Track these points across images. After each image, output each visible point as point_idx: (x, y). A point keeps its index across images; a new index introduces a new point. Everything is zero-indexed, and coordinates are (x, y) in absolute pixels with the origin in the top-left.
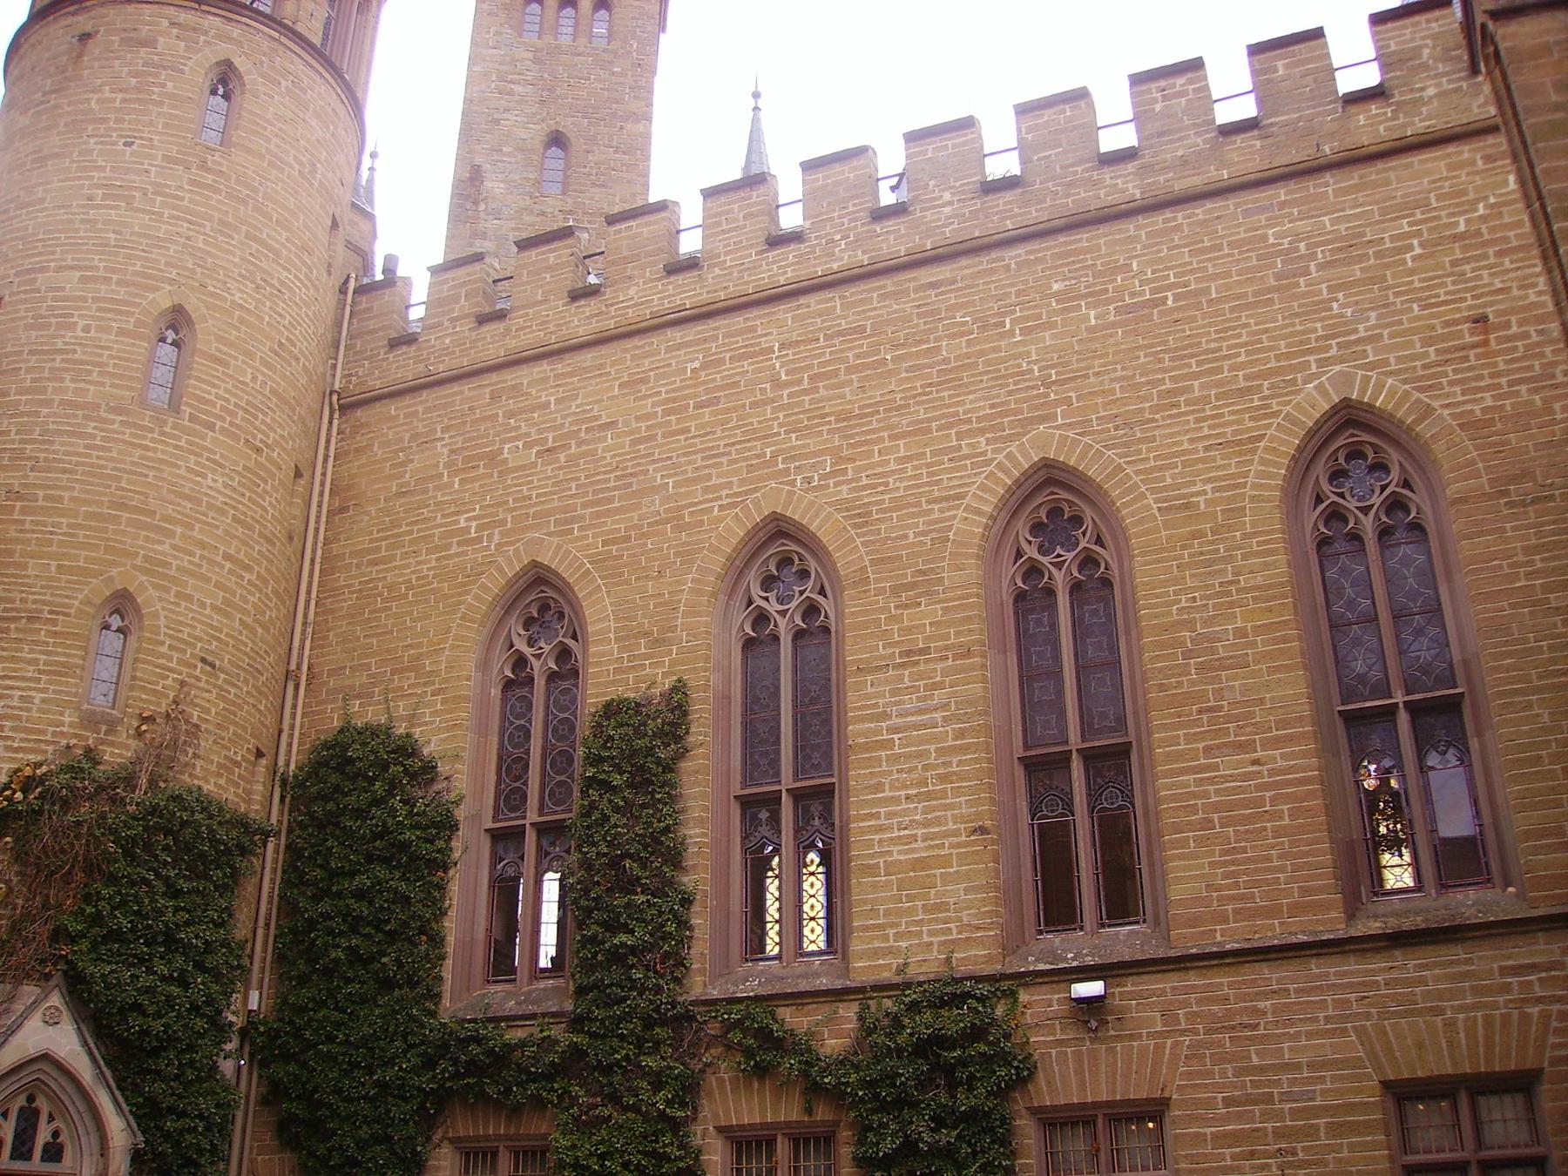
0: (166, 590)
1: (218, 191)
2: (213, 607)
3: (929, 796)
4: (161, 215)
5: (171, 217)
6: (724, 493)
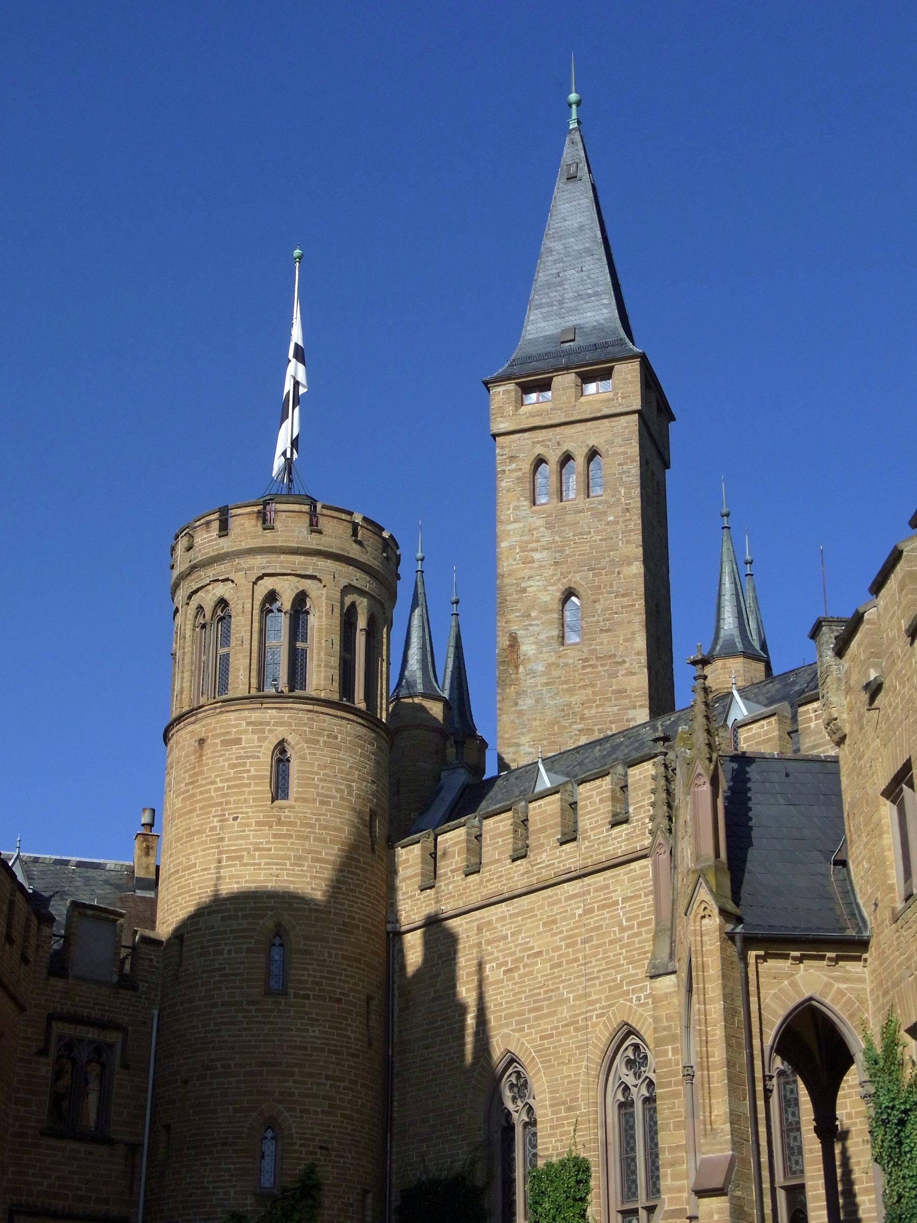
1: (290, 837)
4: (259, 864)
5: (267, 864)
6: (598, 1005)
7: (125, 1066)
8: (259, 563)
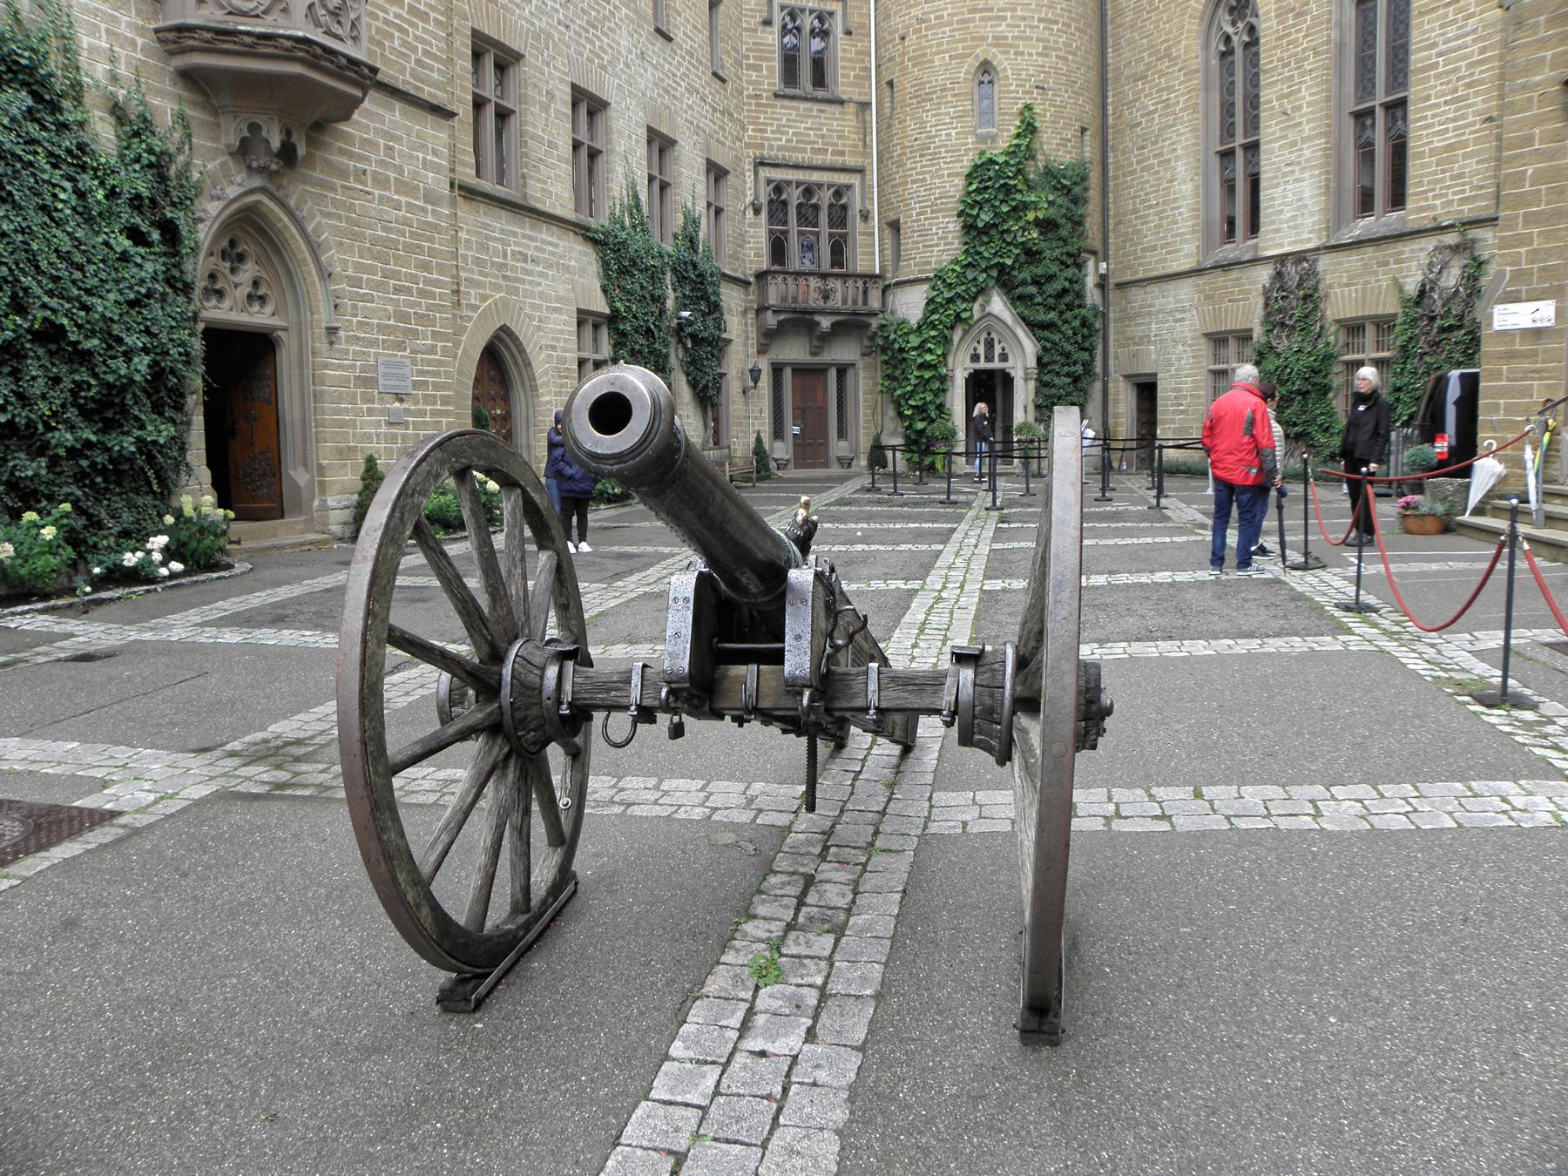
0: (1008, 53)
2: (1038, 54)
3: (1458, 100)
7: (848, 33)
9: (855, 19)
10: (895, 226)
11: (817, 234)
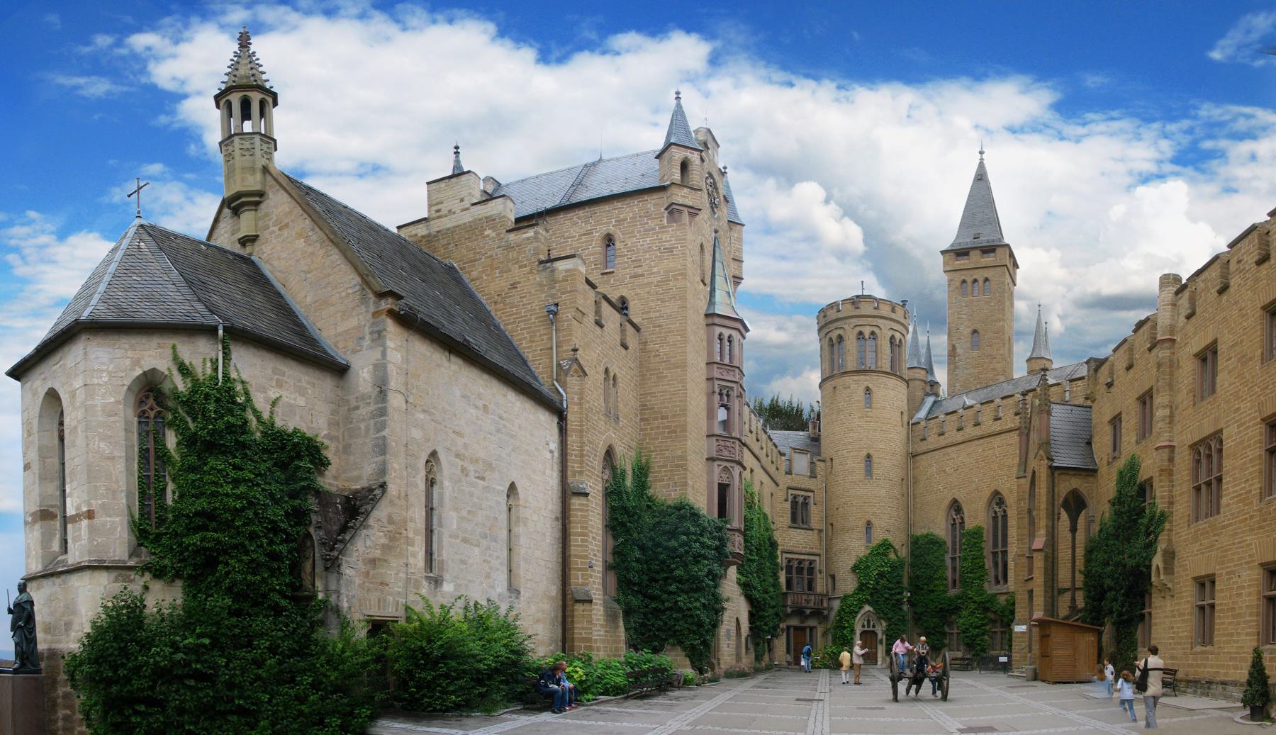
8: (855, 321)
9: (817, 499)
10: (833, 577)
11: (803, 578)
